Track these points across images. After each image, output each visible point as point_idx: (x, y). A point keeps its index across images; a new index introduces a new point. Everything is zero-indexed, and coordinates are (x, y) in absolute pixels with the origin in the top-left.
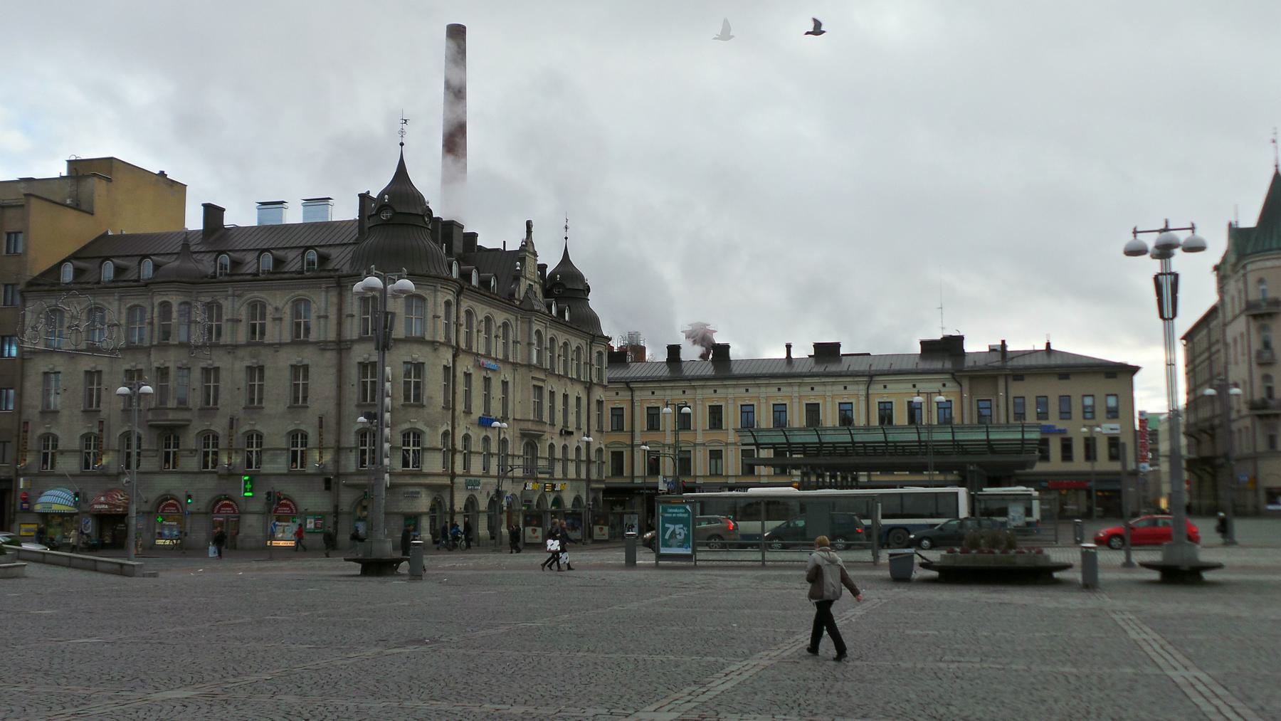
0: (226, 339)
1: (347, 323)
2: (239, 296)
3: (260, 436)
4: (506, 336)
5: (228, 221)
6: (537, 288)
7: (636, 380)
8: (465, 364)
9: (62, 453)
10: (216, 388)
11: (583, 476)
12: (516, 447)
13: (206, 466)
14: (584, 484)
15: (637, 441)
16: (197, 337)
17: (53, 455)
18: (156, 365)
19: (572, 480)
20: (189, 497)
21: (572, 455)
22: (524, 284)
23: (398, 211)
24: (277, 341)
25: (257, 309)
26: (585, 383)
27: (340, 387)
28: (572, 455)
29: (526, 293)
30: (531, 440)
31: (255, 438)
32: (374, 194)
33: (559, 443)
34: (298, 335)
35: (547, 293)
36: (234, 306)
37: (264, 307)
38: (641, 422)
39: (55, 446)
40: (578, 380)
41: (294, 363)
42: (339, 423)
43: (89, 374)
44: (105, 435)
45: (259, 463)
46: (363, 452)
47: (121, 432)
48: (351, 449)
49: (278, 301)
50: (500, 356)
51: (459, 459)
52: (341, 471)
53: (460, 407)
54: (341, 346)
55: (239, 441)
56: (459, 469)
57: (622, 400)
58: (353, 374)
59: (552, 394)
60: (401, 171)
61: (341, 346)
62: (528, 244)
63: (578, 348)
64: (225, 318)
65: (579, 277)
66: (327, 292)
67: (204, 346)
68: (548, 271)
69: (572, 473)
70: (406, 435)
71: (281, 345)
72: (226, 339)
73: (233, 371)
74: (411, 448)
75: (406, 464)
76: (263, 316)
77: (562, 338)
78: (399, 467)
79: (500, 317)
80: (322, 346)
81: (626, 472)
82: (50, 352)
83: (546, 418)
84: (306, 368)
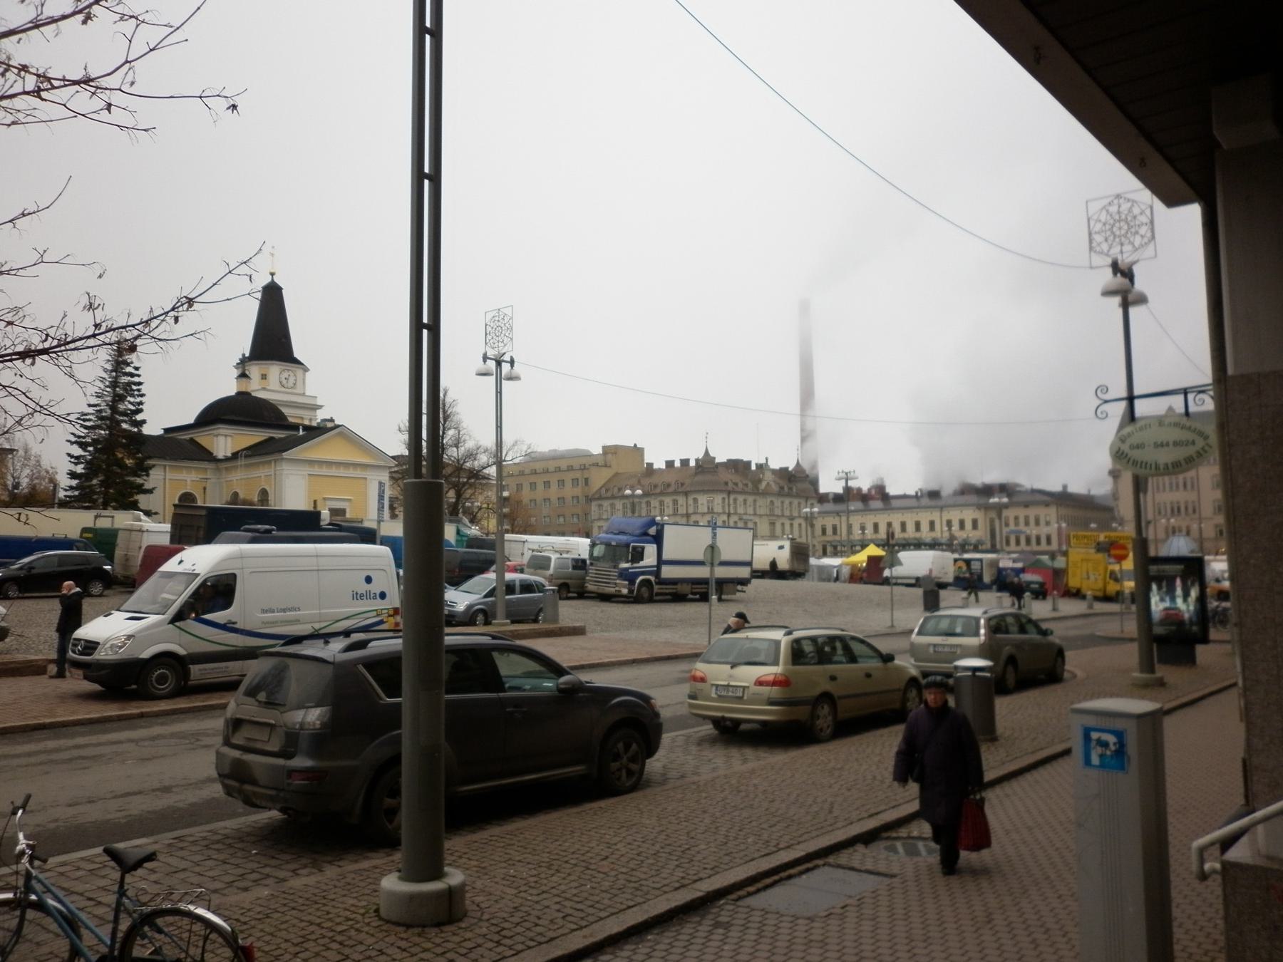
5: (655, 467)
49: (668, 500)
50: (752, 512)
57: (836, 521)
59: (783, 524)
60: (707, 452)
79: (750, 499)
80: (682, 515)
82: (600, 519)
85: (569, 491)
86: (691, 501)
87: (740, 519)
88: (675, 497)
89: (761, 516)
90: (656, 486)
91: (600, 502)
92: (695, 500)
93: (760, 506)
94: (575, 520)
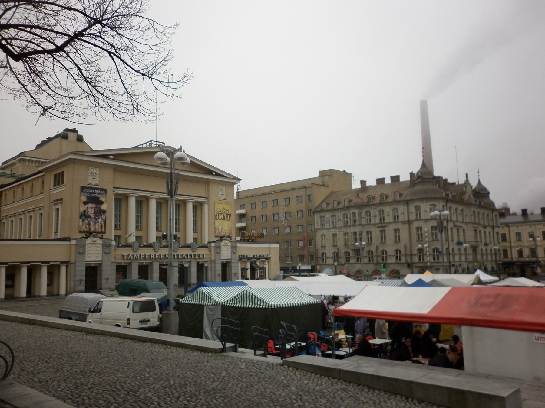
0: (372, 222)
1: (411, 215)
2: (375, 209)
3: (386, 252)
4: (462, 213)
5: (368, 184)
6: (472, 196)
7: (510, 223)
8: (450, 225)
9: (328, 258)
10: (371, 237)
11: (494, 259)
12: (470, 251)
13: (370, 261)
14: (495, 263)
15: (513, 245)
16: (364, 222)
17: (325, 259)
18: (353, 231)
19: (490, 261)
20: (368, 271)
21: (489, 252)
22: (467, 195)
23: (424, 177)
24: (388, 222)
25: (381, 212)
26: (491, 226)
27: (410, 236)
28: (489, 252)
29: (468, 198)
30: (474, 248)
31: (384, 252)
32: (415, 172)
33: (484, 248)
34: (395, 219)
35: (474, 195)
36: (374, 212)
37: (383, 211)
38: (513, 238)
39: (326, 256)
40: (489, 226)
41: (395, 228)
42: (411, 247)
43: (333, 235)
44: (339, 252)
45: (386, 260)
46: (420, 256)
47: (344, 251)
48: (416, 255)
49: (388, 209)
50: (461, 221)
51: (451, 257)
52: (413, 262)
53: (450, 239)
54: (409, 222)
55: (380, 253)
56: (451, 260)
58: (414, 231)
59: (480, 231)
61: (409, 222)
62: (467, 181)
63: (488, 215)
64: (372, 215)
65: (485, 189)
66: (403, 205)
67: (367, 224)
68: (473, 188)
69: (489, 258)
70: (434, 250)
71: (390, 223)
72: (372, 222)
73: (376, 233)
74: (436, 254)
75: (434, 259)
76: (383, 214)
77: (482, 212)
78: (432, 260)
79: (460, 208)
80: (404, 222)
81: (509, 256)
83: (479, 240)
84: (399, 230)
85: (294, 207)
86: (412, 208)
87: (455, 226)
88: (395, 206)
89: (467, 223)
90: (374, 198)
91: (322, 214)
92: (417, 208)
93: (466, 215)
94: (300, 230)
